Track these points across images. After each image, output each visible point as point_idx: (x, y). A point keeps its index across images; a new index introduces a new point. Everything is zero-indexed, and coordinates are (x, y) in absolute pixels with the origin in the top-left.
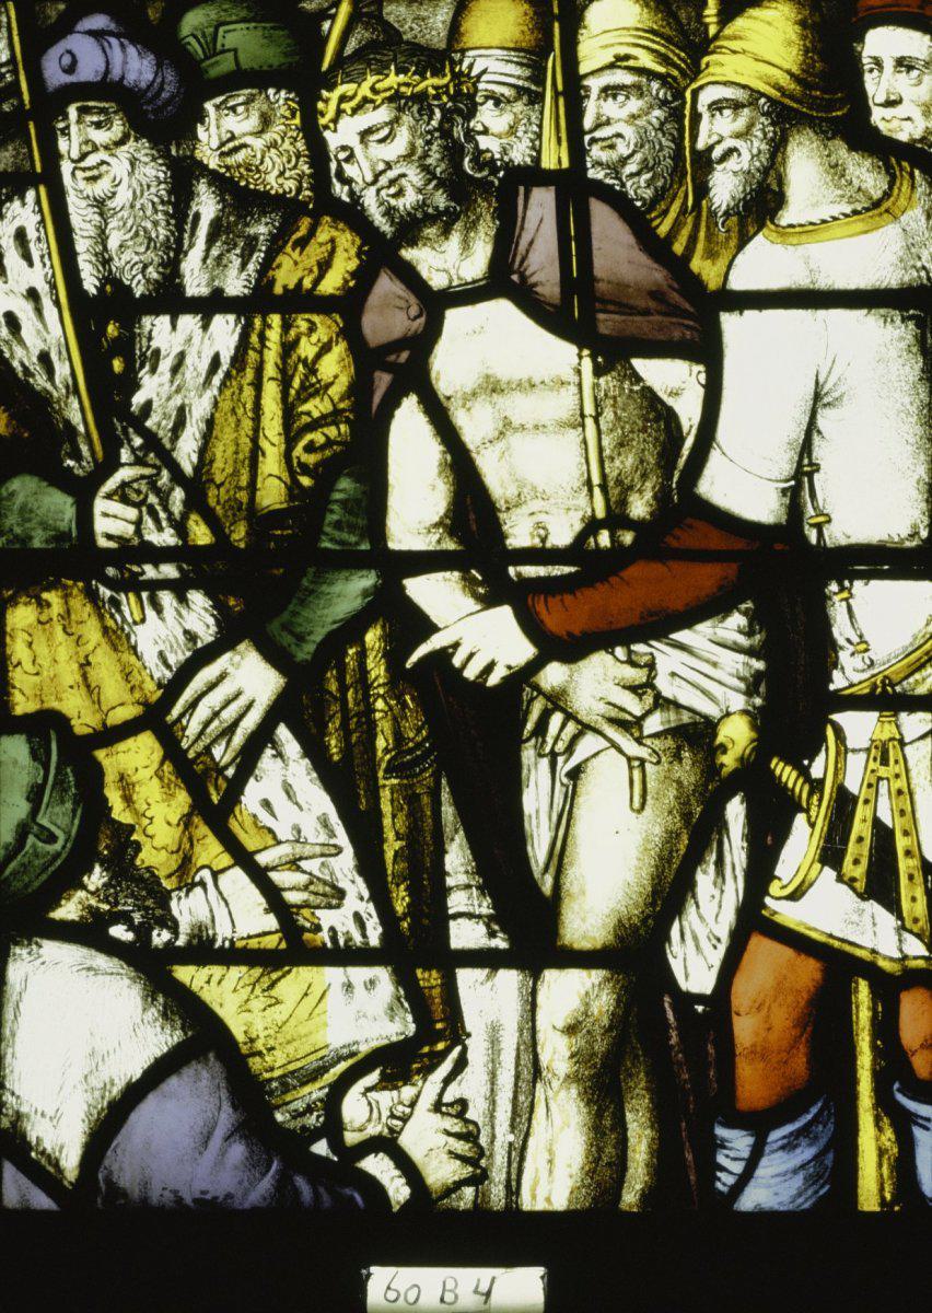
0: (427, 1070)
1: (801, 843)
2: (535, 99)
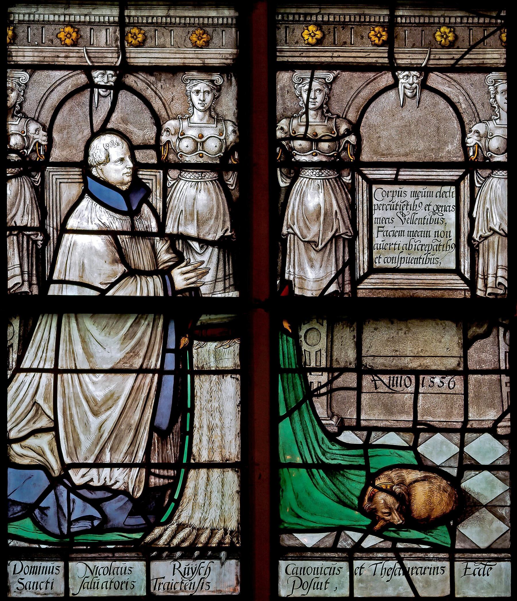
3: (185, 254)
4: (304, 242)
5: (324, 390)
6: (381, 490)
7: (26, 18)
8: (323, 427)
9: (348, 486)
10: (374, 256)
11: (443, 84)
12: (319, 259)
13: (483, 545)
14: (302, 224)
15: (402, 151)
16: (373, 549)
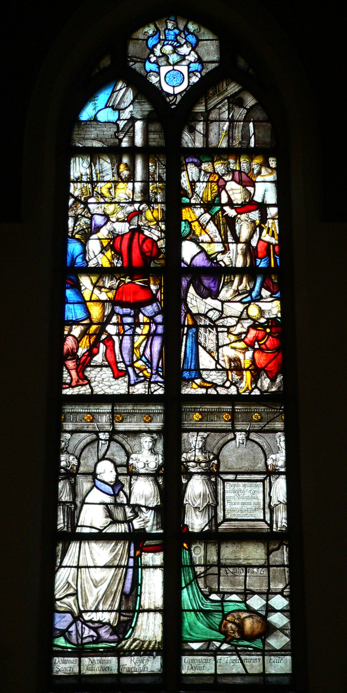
0: (226, 254)
1: (265, 231)
2: (236, 163)
3: (139, 513)
4: (194, 507)
5: (202, 575)
6: (229, 622)
7: (70, 411)
8: (202, 592)
9: (214, 620)
10: (226, 513)
11: (256, 438)
12: (201, 515)
13: (278, 648)
14: (192, 500)
15: (238, 467)
16: (226, 650)
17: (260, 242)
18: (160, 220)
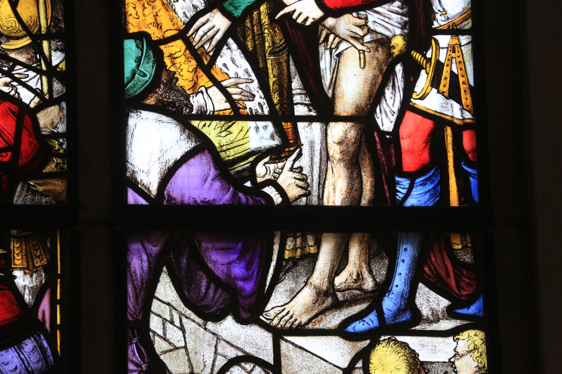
0: (287, 158)
17: (410, 116)
18: (44, 30)
